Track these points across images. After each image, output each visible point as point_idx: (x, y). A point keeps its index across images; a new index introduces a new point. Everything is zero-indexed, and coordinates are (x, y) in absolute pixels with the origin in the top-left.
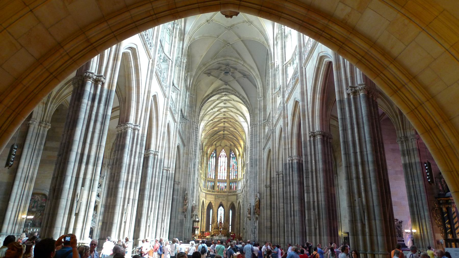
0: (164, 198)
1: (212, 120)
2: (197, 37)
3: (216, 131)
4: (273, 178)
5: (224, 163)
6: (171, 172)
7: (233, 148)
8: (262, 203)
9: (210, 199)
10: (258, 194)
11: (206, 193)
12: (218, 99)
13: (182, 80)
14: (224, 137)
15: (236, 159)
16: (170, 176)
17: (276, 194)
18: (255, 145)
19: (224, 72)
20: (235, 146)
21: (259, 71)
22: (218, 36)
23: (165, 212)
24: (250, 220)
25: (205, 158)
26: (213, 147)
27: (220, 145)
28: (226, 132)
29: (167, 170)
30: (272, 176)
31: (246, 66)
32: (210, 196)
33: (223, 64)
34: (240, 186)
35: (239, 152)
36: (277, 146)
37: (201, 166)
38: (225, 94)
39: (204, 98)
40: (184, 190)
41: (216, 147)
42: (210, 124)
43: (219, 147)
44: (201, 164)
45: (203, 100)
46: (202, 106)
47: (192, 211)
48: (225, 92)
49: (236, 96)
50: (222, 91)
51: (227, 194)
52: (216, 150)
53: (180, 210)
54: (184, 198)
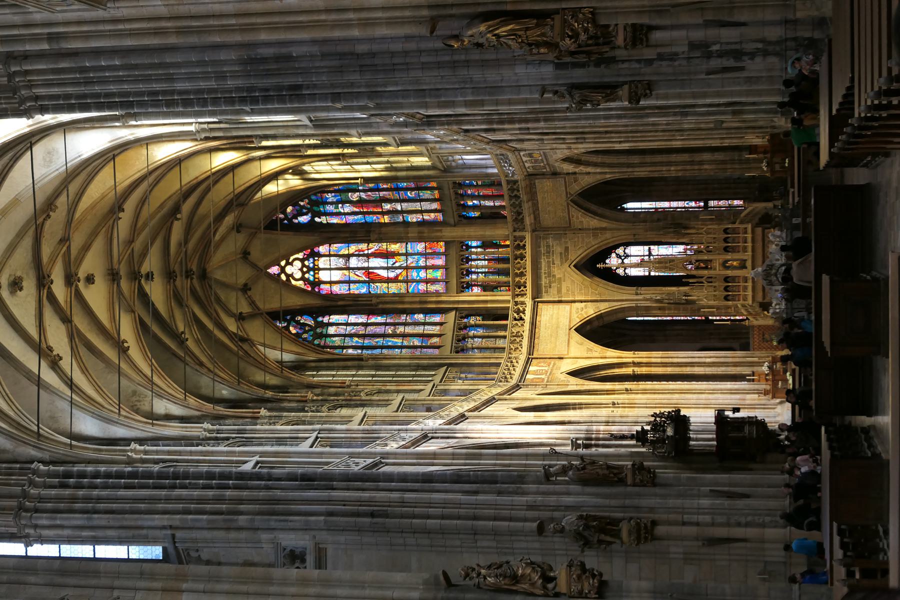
1: (55, 364)
3: (142, 327)
5: (354, 262)
14: (188, 274)
18: (147, 79)
24: (648, 88)
25: (325, 376)
26: (256, 330)
27: (245, 289)
28: (152, 263)
35: (275, 176)
37: (363, 404)
41: (256, 314)
42: (84, 370)
43: (256, 293)
52: (274, 315)
54: (497, 590)
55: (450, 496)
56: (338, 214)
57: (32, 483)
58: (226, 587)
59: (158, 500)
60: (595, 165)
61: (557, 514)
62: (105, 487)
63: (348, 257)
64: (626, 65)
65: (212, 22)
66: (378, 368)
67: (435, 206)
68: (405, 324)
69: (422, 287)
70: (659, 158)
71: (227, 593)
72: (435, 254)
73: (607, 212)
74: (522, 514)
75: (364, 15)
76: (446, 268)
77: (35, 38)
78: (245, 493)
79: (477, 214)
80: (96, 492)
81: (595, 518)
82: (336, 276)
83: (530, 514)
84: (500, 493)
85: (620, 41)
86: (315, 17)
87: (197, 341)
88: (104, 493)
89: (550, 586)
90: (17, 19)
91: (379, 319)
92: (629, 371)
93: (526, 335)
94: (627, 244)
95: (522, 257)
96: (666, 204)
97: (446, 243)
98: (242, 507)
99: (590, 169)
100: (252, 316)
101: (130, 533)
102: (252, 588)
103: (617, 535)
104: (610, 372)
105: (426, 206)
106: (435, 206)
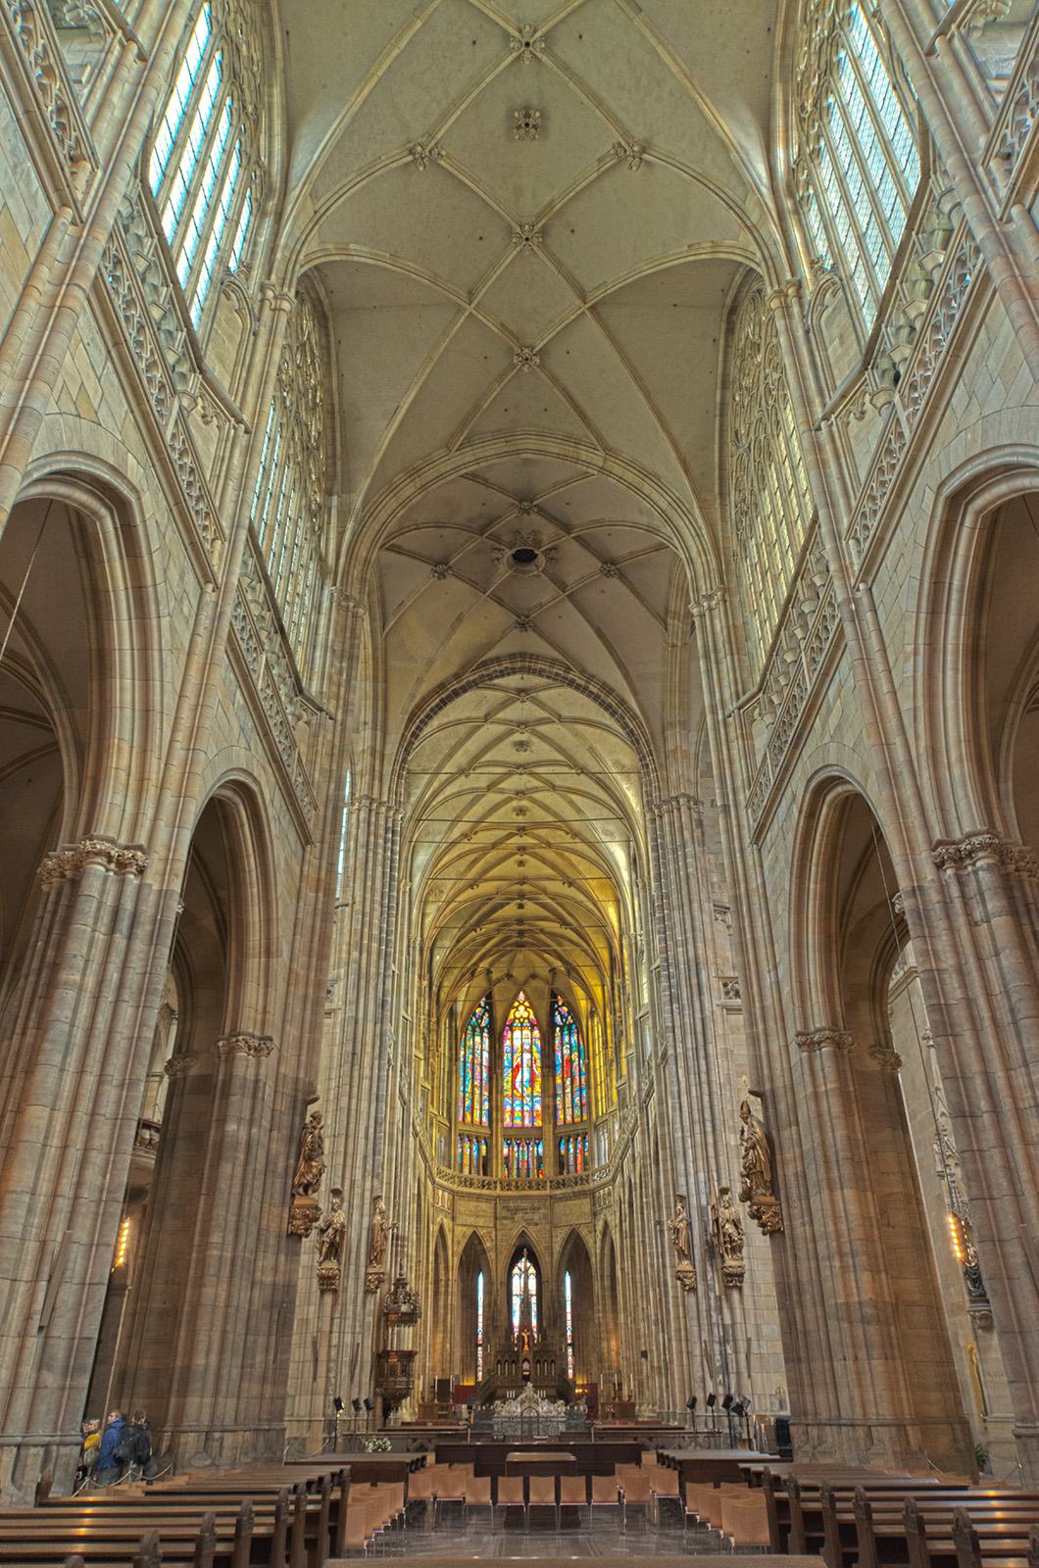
0: (81, 1072)
1: (465, 836)
2: (360, 253)
4: (917, 891)
5: (527, 1056)
6: (152, 879)
7: (559, 984)
8: (788, 1153)
9: (476, 1217)
10: (756, 1105)
11: (453, 1193)
12: (487, 718)
13: (263, 382)
14: (521, 933)
15: (579, 1032)
16: (148, 910)
17: (969, 1002)
18: (679, 891)
19: (509, 553)
20: (572, 970)
21: (687, 471)
22: (471, 294)
23: (79, 1184)
25: (445, 1034)
26: (480, 982)
27: (509, 976)
28: (531, 908)
29: (122, 865)
30: (903, 884)
31: (617, 470)
32: (473, 1204)
33: (502, 490)
34: (604, 1146)
35: (590, 997)
36: (908, 670)
37: (427, 1059)
38: (522, 692)
39: (425, 700)
40: (305, 1096)
42: (460, 857)
44: (427, 1049)
45: (419, 707)
46: (415, 735)
47: (374, 1255)
48: (522, 670)
49: (571, 683)
50: (506, 665)
51: (548, 1192)
52: (489, 996)
53: (275, 1220)
54: (301, 1144)
55: (364, 1117)
56: (562, 1045)
57: (389, 809)
58: (318, 925)
59: (373, 895)
60: (602, 1248)
61: (346, 1205)
62: (384, 858)
63: (531, 1052)
64: (709, 1268)
65: (747, 921)
66: (450, 1073)
67: (569, 1118)
68: (481, 1095)
69: (508, 1108)
70: (608, 1302)
71: (313, 927)
72: (533, 1119)
73: (565, 1258)
74: (348, 1175)
75: (762, 1037)
76: (522, 1127)
77: (724, 795)
78: (374, 957)
79: (563, 1152)
80: (380, 851)
81: (342, 1238)
82: (517, 1044)
83: (347, 1182)
84: (365, 1157)
85: (730, 1261)
86: (757, 999)
87: (474, 939)
88: (380, 857)
89: (301, 1190)
90: (739, 783)
91: (485, 1075)
92: (442, 1277)
93: (472, 1190)
94: (539, 1276)
95: (530, 1188)
96: (569, 1309)
97: (541, 1128)
98: (365, 955)
99: (599, 1243)
100: (489, 980)
101: (351, 874)
102: (316, 945)
103: (327, 1258)
104: (441, 1260)
105: (569, 1111)
106: (569, 1118)
